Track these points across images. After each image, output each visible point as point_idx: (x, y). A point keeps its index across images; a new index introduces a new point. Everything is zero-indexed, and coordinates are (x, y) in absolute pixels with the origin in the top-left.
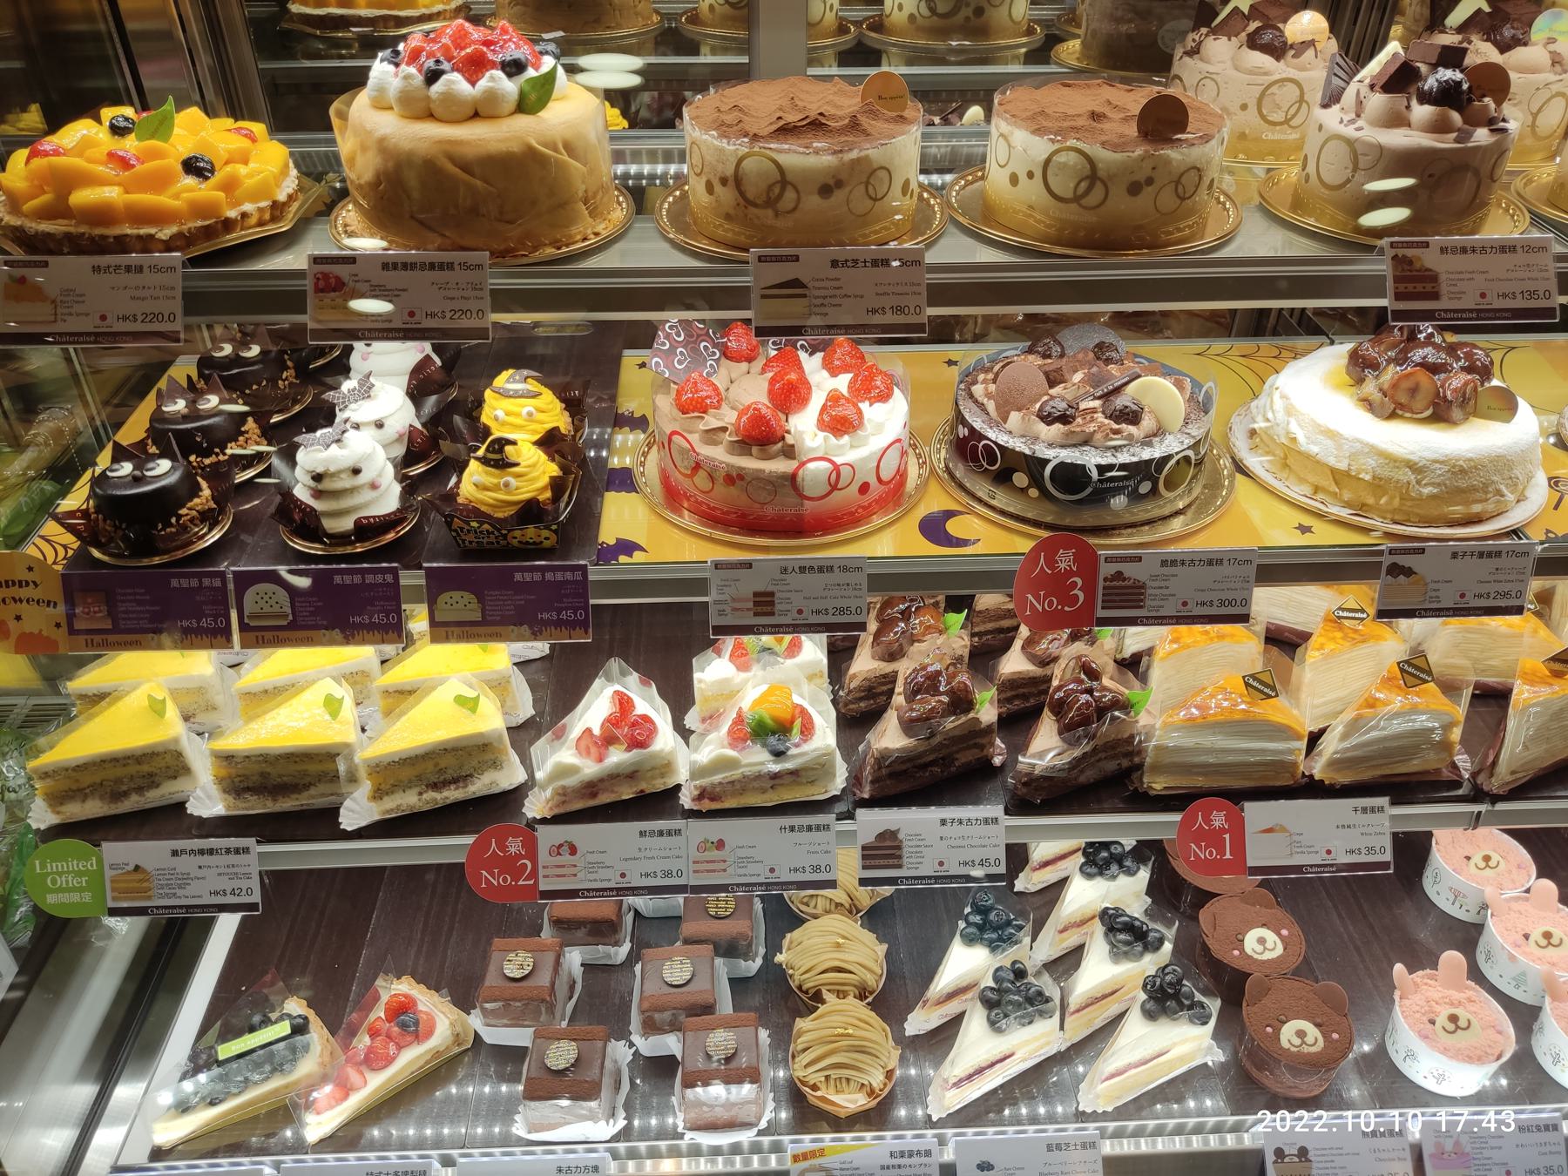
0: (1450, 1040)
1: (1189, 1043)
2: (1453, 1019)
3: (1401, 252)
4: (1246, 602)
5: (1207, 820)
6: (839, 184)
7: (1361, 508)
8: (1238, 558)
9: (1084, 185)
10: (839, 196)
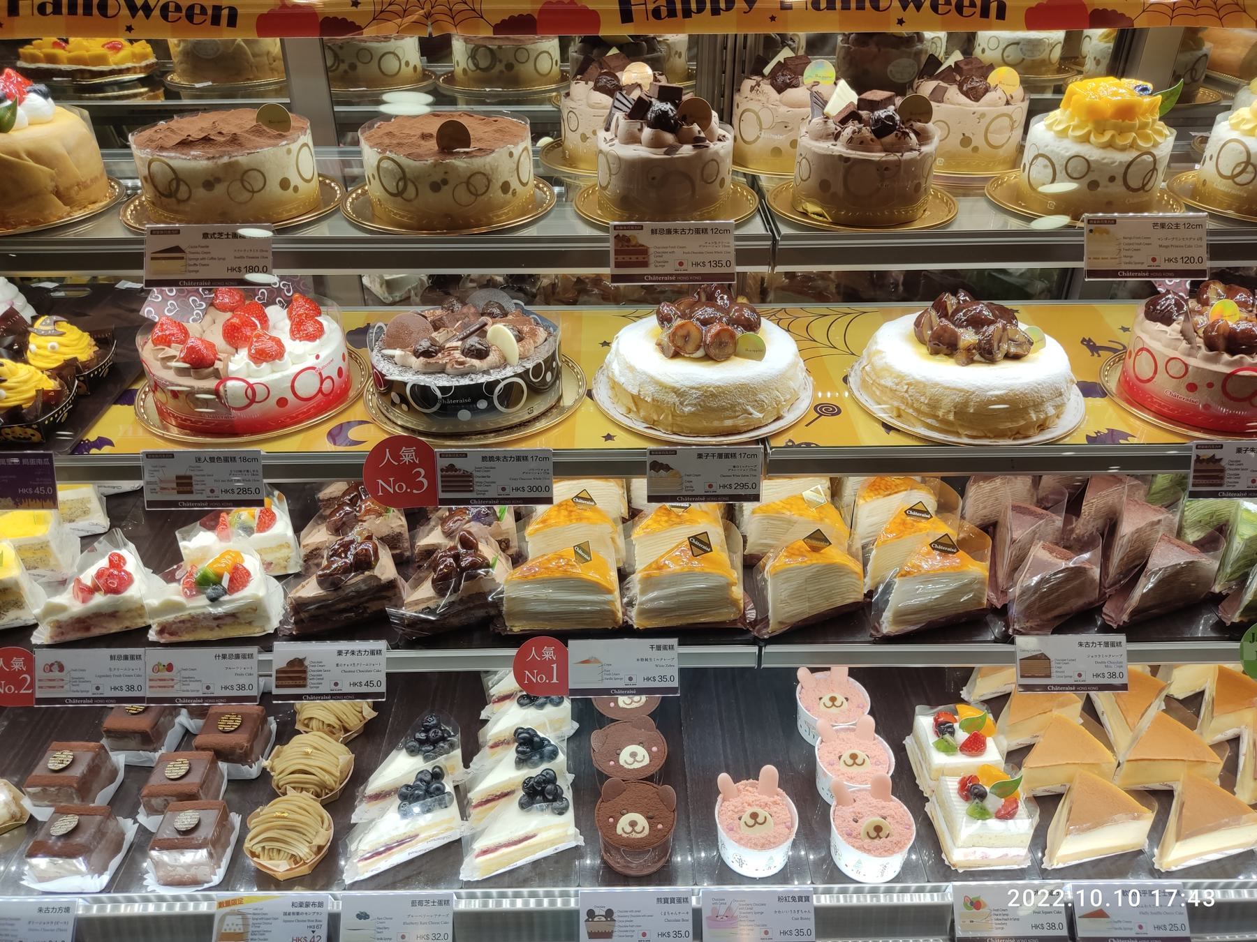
0: (745, 831)
1: (555, 830)
2: (754, 816)
3: (621, 233)
4: (549, 489)
5: (540, 654)
6: (218, 180)
7: (653, 424)
8: (542, 456)
9: (401, 184)
10: (220, 189)
